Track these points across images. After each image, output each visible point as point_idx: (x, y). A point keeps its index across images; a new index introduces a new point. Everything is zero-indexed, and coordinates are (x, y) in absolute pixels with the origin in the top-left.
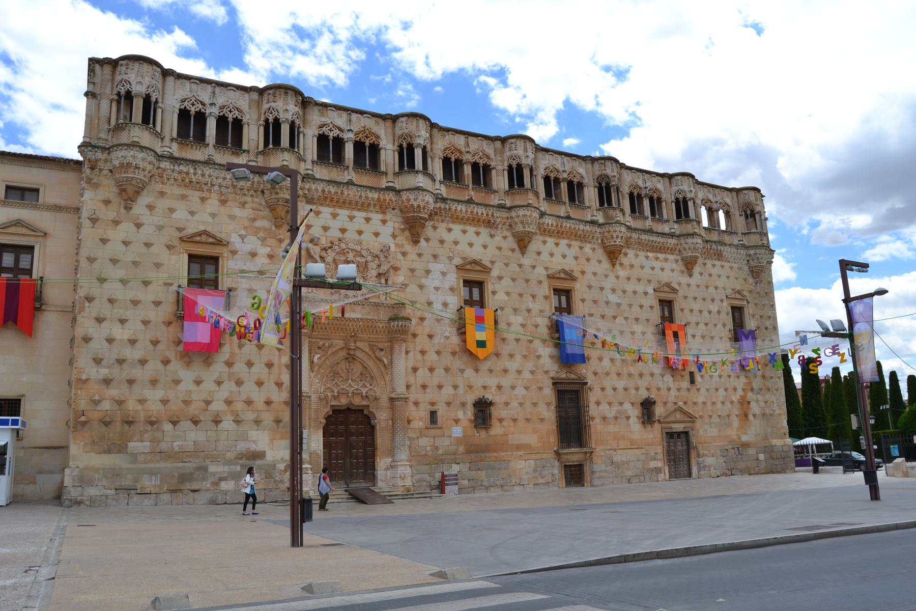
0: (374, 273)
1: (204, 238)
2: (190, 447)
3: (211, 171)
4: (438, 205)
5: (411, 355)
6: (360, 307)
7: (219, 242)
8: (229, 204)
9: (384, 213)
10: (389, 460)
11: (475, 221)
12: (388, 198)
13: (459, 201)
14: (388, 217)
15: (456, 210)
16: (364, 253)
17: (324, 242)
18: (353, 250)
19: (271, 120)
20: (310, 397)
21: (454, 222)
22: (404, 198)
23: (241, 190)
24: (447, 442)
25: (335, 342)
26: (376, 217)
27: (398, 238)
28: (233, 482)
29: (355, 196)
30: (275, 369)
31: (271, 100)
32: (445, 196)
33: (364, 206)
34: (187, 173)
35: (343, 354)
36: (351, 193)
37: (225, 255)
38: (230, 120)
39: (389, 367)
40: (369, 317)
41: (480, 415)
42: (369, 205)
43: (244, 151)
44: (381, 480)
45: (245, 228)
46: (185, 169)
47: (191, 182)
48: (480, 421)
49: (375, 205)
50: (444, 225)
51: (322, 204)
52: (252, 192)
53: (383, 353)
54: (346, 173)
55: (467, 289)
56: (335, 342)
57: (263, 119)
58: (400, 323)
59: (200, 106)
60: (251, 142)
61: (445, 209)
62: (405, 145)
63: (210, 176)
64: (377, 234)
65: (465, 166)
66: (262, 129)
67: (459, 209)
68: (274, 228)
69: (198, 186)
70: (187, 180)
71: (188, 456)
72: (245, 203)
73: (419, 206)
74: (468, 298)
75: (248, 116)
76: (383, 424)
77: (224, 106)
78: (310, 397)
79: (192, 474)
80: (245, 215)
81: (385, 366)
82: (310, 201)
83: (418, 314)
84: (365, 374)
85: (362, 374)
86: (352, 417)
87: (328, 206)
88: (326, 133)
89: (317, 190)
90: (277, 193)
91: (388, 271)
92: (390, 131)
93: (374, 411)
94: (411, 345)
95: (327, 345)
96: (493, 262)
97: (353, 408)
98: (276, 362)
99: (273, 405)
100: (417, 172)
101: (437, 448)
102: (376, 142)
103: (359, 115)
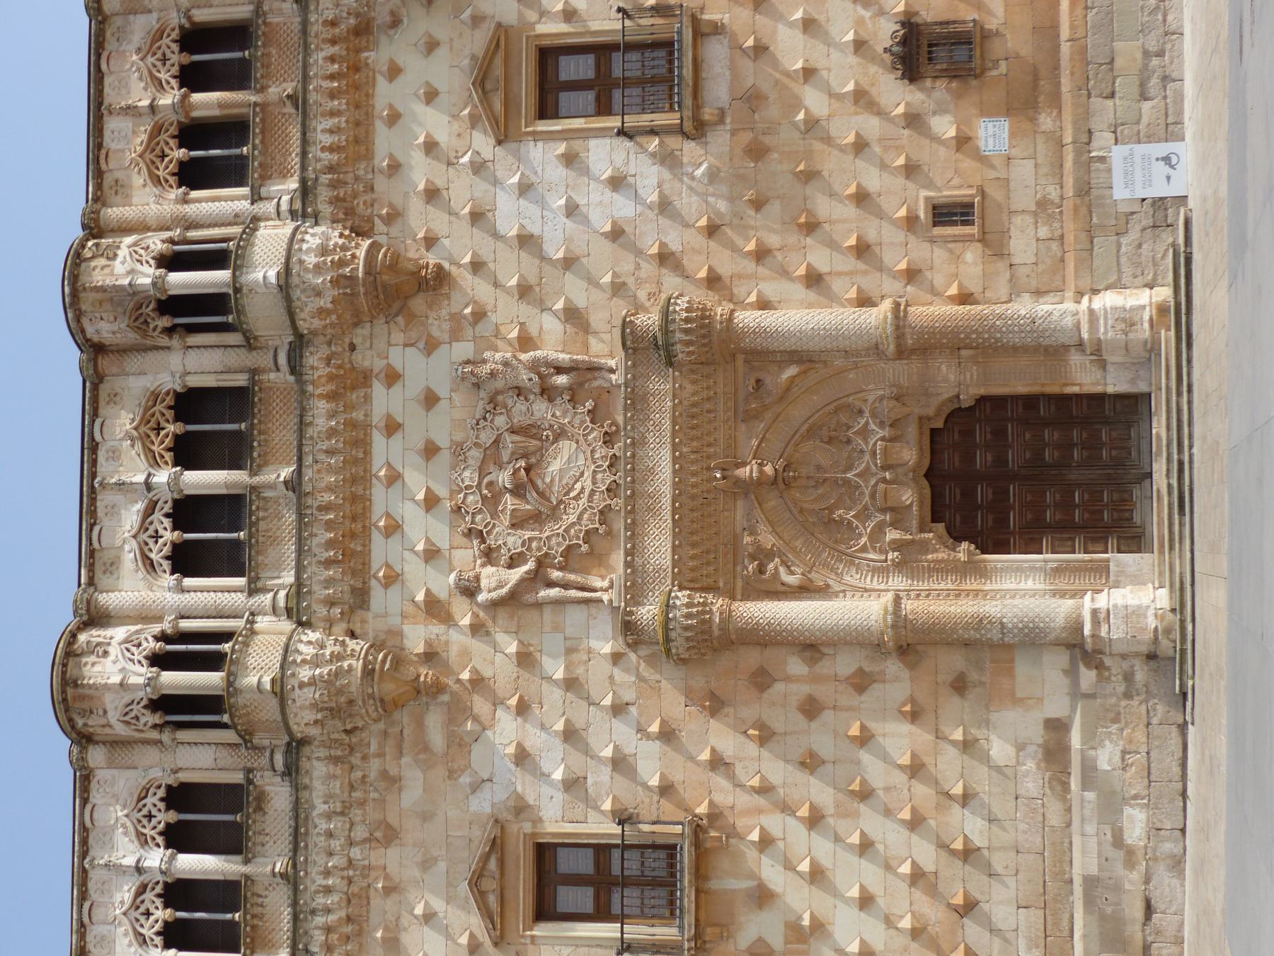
0: (541, 409)
1: (489, 885)
2: (1036, 915)
3: (314, 871)
4: (326, 210)
7: (497, 845)
8: (393, 819)
9: (365, 378)
10: (1075, 358)
11: (355, 80)
12: (324, 371)
13: (305, 142)
14: (379, 365)
15: (331, 149)
16: (487, 438)
19: (157, 718)
21: (369, 156)
22: (317, 323)
23: (352, 787)
24: (1023, 172)
26: (383, 401)
27: (435, 332)
28: (1128, 811)
29: (331, 469)
30: (823, 692)
31: (103, 721)
32: (293, 184)
33: (356, 440)
34: (328, 930)
36: (324, 480)
37: (528, 827)
38: (172, 816)
40: (667, 424)
41: (941, 53)
42: (352, 425)
43: (250, 782)
44: (1133, 381)
45: (452, 774)
46: (319, 937)
47: (349, 919)
48: (961, 53)
49: (349, 407)
50: (381, 184)
51: (366, 564)
52: (356, 760)
53: (768, 380)
54: (268, 494)
55: (564, 97)
57: (155, 735)
58: (678, 335)
59: (149, 896)
60: (221, 764)
61: (333, 185)
62: (165, 322)
63: (327, 873)
64: (430, 400)
65: (195, 114)
66: (183, 735)
67: (327, 140)
69: (357, 900)
70: (348, 929)
71: (1056, 924)
72: (384, 774)
73: (335, 282)
74: (590, 96)
75: (156, 773)
76: (973, 373)
77: (140, 835)
79: (1103, 917)
80: (418, 774)
82: (361, 598)
84: (833, 430)
85: (830, 441)
87: (367, 545)
88: (167, 550)
89: (328, 582)
90: (351, 702)
92: (134, 362)
93: (935, 402)
96: (477, 20)
97: (927, 462)
98: (806, 689)
100: (237, 290)
101: (1043, 204)
102: (170, 401)
103: (101, 454)
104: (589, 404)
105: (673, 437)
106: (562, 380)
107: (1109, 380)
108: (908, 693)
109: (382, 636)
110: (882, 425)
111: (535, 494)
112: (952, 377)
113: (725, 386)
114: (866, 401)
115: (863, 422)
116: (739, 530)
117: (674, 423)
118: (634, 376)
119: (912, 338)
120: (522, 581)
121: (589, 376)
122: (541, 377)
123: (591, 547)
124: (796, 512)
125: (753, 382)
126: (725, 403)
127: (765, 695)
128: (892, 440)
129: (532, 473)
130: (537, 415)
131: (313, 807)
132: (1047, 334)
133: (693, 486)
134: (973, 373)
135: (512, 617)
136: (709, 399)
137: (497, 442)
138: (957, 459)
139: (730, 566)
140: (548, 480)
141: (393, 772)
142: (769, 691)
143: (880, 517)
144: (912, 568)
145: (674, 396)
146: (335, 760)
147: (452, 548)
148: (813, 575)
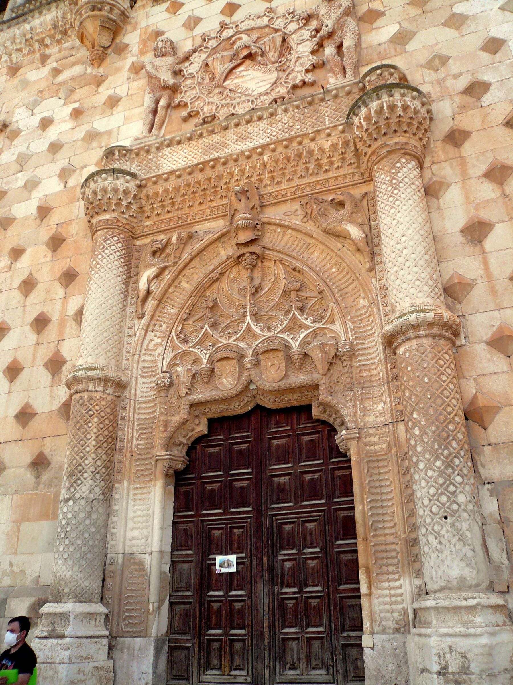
5: (453, 196)
6: (262, 124)
10: (406, 585)
16: (279, 24)
17: (187, 46)
18: (249, 31)
20: (121, 386)
25: (201, 228)
30: (52, 331)
35: (226, 252)
39: (371, 247)
53: (345, 212)
56: (201, 228)
68: (89, 70)
78: (121, 386)
81: (359, 250)
83: (463, 83)
86: (279, 436)
91: (340, 25)
94: (446, 171)
95: (174, 239)
97: (269, 403)
99: (34, 423)
104: (309, 78)
105: (279, 142)
106: (329, 50)
107: (379, 639)
108: (39, 410)
109: (133, 21)
110: (305, 343)
111: (230, 68)
112: (371, 419)
113: (336, 178)
114: (333, 322)
115: (308, 323)
116: (195, 228)
117: (291, 140)
118: (336, 97)
119: (406, 351)
120: (158, 79)
121: (337, 71)
122: (331, 35)
123: (185, 120)
124: (214, 275)
125: (340, 198)
126: (317, 183)
127: (57, 283)
128: (289, 359)
129: (248, 62)
130: (300, 48)
131: (29, 23)
132: (431, 538)
133: (231, 174)
134: (378, 443)
135: (139, 89)
136: (320, 166)
137: (276, 31)
138: (281, 441)
139: (163, 227)
140: (243, 73)
141: (49, 61)
142: (59, 285)
143: (204, 358)
144: (154, 400)
145: (318, 132)
146: (55, 26)
147: (193, 37)
148: (151, 304)
